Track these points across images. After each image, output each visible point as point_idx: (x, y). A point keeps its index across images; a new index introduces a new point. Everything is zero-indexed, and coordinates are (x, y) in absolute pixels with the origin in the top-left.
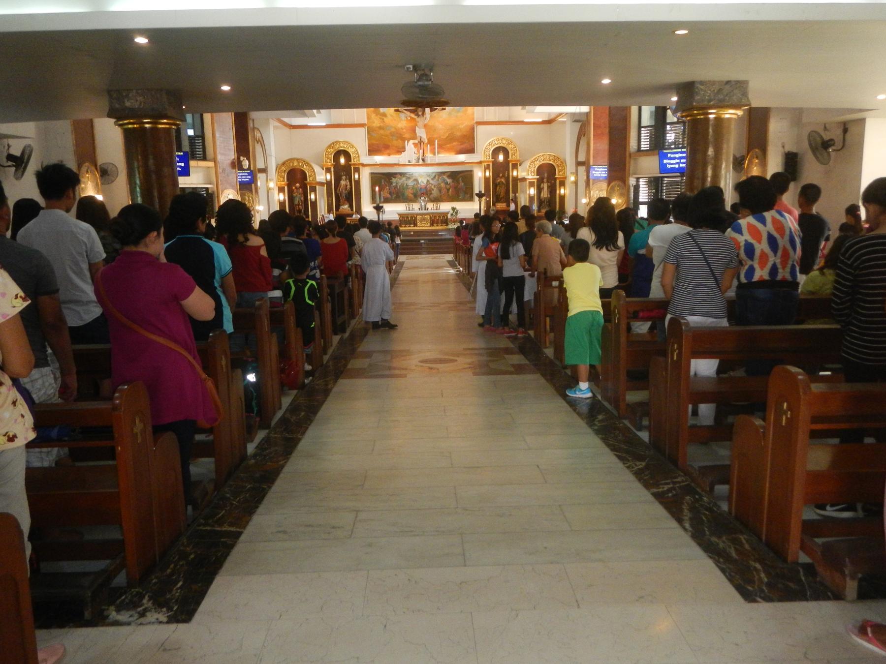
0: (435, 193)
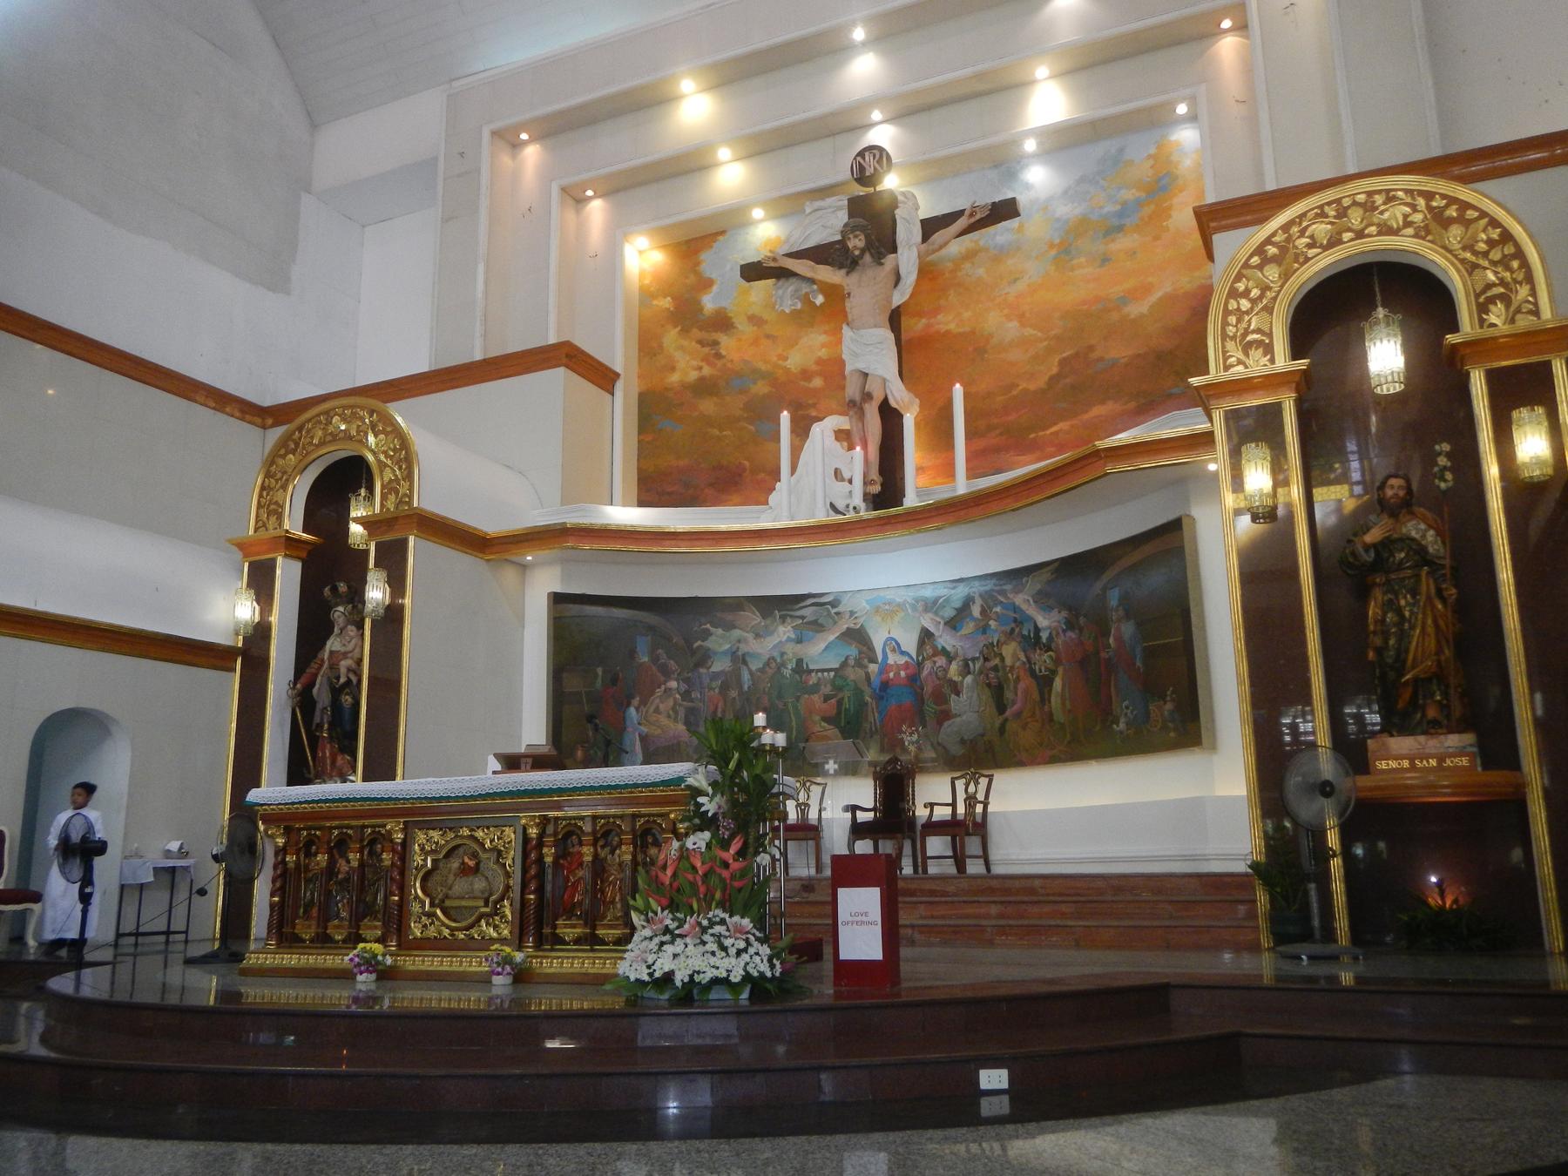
0: (968, 709)
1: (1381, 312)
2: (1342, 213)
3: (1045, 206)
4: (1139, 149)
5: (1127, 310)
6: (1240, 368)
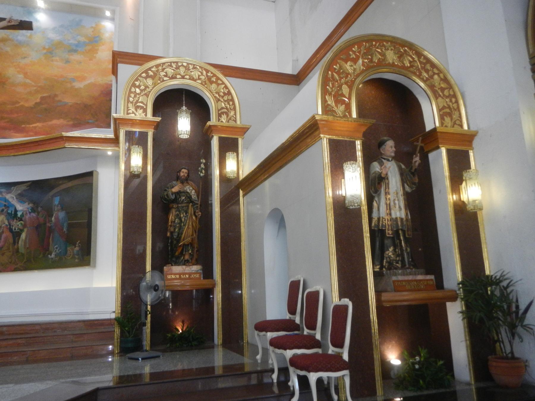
1: (184, 108)
2: (178, 68)
3: (44, 31)
4: (88, 23)
5: (74, 84)
6: (133, 115)
